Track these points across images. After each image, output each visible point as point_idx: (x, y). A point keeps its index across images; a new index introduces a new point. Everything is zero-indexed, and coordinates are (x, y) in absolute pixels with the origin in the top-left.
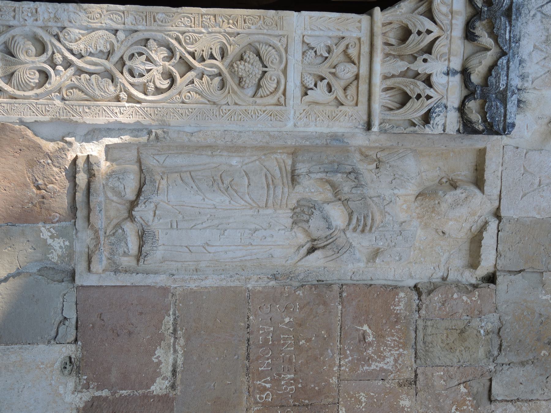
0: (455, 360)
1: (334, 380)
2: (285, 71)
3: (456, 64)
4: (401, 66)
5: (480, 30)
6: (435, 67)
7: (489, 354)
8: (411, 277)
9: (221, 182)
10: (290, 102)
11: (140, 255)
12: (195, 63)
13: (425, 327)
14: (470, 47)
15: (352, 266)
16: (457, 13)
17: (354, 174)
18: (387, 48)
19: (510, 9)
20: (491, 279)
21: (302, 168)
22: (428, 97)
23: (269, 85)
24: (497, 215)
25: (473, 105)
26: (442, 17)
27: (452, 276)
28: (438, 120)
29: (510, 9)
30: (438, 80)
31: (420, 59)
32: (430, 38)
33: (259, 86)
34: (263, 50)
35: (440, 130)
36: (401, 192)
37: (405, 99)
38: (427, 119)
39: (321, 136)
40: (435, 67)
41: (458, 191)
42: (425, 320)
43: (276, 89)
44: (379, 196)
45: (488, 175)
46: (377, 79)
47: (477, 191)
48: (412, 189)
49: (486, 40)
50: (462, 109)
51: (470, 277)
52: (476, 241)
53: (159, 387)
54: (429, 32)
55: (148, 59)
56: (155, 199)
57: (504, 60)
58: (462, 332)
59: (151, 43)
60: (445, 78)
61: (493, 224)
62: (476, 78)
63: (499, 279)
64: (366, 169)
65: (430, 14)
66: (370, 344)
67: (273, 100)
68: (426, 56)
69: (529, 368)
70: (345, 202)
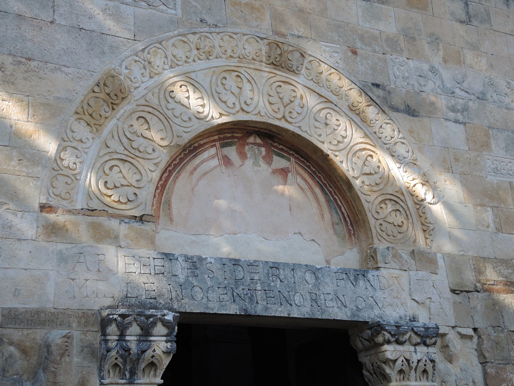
0: (506, 347)
3: (412, 348)
5: (402, 339)
6: (415, 358)
7: (502, 332)
8: (477, 365)
13: (498, 360)
14: (407, 343)
16: (395, 348)
18: (406, 379)
19: (396, 326)
20: (475, 330)
22: (426, 361)
24: (453, 327)
25: (428, 341)
26: (397, 355)
27: (475, 347)
28: (433, 356)
29: (396, 326)
30: (419, 356)
35: (435, 355)
36: (452, 370)
37: (425, 371)
38: (432, 361)
40: (415, 358)
41: (450, 345)
42: (495, 360)
44: (456, 381)
47: (448, 336)
48: (449, 365)
49: (407, 337)
51: (475, 339)
54: (403, 361)
57: (415, 329)
58: (497, 343)
60: (418, 353)
62: (419, 340)
63: (476, 327)
65: (395, 361)
68: (411, 363)
69: (504, 314)
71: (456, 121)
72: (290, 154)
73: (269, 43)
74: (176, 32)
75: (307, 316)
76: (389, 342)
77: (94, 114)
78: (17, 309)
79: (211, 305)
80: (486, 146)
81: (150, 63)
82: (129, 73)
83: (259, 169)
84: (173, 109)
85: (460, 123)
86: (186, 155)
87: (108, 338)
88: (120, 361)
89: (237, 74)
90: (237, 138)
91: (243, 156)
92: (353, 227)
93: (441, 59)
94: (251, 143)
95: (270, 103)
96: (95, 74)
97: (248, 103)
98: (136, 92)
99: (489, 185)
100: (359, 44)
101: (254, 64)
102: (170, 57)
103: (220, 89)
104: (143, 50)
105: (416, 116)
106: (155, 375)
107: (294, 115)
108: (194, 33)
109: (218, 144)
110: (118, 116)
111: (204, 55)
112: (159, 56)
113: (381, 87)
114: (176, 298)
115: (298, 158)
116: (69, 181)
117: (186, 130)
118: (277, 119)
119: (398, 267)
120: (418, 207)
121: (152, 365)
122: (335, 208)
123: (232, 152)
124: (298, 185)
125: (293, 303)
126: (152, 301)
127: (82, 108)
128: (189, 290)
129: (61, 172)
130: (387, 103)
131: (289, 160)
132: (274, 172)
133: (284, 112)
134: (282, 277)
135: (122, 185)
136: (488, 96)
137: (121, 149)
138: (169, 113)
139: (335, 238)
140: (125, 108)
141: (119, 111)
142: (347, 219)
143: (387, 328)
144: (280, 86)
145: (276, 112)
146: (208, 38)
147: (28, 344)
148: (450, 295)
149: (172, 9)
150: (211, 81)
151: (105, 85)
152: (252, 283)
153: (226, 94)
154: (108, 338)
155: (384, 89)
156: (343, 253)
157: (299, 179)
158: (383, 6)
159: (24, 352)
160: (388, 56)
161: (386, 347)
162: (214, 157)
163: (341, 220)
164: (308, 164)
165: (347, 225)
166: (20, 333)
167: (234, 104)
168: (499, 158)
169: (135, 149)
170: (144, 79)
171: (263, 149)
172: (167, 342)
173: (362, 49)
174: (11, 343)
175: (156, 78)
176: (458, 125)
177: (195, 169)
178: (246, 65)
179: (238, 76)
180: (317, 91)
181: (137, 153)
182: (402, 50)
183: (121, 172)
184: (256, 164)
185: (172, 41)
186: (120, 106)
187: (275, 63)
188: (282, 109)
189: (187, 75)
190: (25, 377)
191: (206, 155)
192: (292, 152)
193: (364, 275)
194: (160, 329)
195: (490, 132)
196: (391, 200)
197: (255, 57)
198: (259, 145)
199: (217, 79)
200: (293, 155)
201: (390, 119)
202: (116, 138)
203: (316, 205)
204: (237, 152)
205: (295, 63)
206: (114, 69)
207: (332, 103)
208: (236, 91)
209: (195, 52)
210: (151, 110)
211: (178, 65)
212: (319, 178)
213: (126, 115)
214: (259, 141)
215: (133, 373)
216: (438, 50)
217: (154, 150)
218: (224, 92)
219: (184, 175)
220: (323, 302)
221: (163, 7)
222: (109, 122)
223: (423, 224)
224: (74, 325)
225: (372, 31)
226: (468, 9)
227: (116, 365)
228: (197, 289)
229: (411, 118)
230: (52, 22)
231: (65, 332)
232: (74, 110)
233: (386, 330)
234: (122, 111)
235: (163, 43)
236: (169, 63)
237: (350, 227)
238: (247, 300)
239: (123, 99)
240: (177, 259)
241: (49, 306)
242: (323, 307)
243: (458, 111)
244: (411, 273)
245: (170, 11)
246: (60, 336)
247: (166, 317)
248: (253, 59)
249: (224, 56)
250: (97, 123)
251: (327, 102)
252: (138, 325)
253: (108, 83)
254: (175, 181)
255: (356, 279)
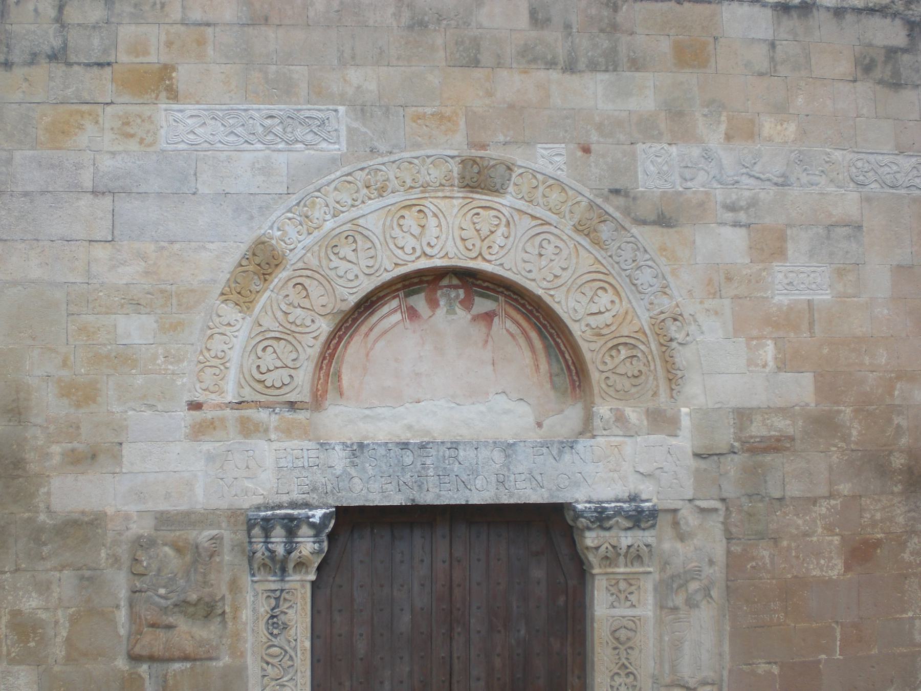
1: (774, 581)
2: (623, 617)
4: (622, 559)
5: (607, 525)
7: (761, 501)
9: (677, 646)
10: (639, 613)
11: (713, 684)
12: (621, 663)
15: (717, 572)
17: (673, 578)
21: (671, 604)
23: (631, 625)
24: (690, 500)
27: (721, 519)
31: (619, 551)
32: (610, 547)
33: (631, 630)
34: (613, 629)
39: (655, 597)
43: (633, 621)
45: (672, 507)
46: (628, 570)
48: (679, 545)
50: (644, 529)
52: (702, 510)
53: (775, 670)
55: (620, 685)
56: (686, 678)
59: (613, 683)
61: (698, 503)
62: (629, 525)
64: (669, 571)
65: (597, 548)
66: (757, 564)
67: (637, 622)
69: (767, 478)
70: (687, 581)
71: (736, 224)
72: (498, 292)
73: (462, 161)
74: (338, 174)
75: (490, 502)
76: (589, 529)
77: (242, 292)
78: (168, 512)
79: (371, 496)
80: (780, 253)
81: (307, 217)
82: (282, 235)
83: (454, 317)
84: (336, 268)
85: (741, 226)
86: (361, 314)
87: (253, 540)
88: (268, 561)
89: (418, 208)
90: (427, 282)
91: (433, 304)
92: (578, 377)
93: (723, 136)
94: (445, 287)
95: (463, 240)
96: (242, 245)
97: (432, 244)
98: (291, 255)
99: (775, 309)
100: (594, 137)
101: (443, 190)
102: (332, 204)
103: (397, 232)
104: (298, 204)
105: (672, 227)
106: (307, 573)
107: (496, 248)
108: (362, 169)
109: (401, 294)
110: (271, 287)
111: (376, 192)
112: (318, 206)
113: (623, 193)
114: (332, 491)
115: (509, 297)
116: (218, 372)
117: (351, 291)
118: (471, 259)
119: (621, 433)
120: (664, 349)
121: (301, 565)
122: (556, 356)
123: (419, 302)
124: (507, 330)
125: (473, 488)
126: (304, 496)
127: (229, 287)
128: (346, 482)
129: (207, 364)
130: (629, 215)
131: (496, 300)
132: (475, 319)
133: (481, 248)
134: (460, 459)
135: (277, 368)
136: (793, 179)
137: (274, 326)
138: (332, 274)
139: (552, 394)
140: (280, 276)
141: (272, 282)
142: (572, 368)
143: (585, 515)
144: (478, 214)
145: (470, 250)
146: (381, 171)
147: (181, 544)
148: (692, 463)
149: (335, 143)
150: (384, 224)
151: (254, 254)
152: (423, 468)
153: (403, 237)
154: (253, 540)
155: (627, 195)
156: (562, 411)
157: (509, 324)
158: (637, 74)
159: (179, 550)
160: (640, 147)
161: (588, 534)
162: (396, 311)
163: (562, 370)
164: (522, 302)
165: (571, 375)
166: (173, 535)
167: (414, 249)
168: (796, 269)
169: (291, 323)
170: (301, 238)
171: (461, 292)
172: (314, 543)
173: (598, 143)
174: (165, 544)
175: (316, 233)
176: (738, 230)
177: (371, 329)
178: (433, 194)
179: (420, 211)
180: (530, 211)
181: (293, 328)
182: (661, 134)
183: (275, 352)
184: (451, 311)
185: (333, 185)
186: (273, 275)
187: (472, 184)
188: (478, 243)
189: (354, 222)
190: (180, 575)
191: (385, 309)
192: (501, 289)
193: (572, 447)
194: (305, 530)
195: (789, 232)
196: (626, 344)
197: (444, 182)
198: (456, 287)
199: (392, 220)
200: (502, 293)
201: (633, 236)
202: (270, 313)
203: (530, 354)
204: (426, 300)
205: (498, 181)
206: (264, 234)
207: (550, 224)
208: (416, 230)
209: (365, 191)
210: (309, 273)
211: (343, 212)
212: (537, 319)
213: (280, 284)
214: (455, 281)
215: (284, 570)
216: (719, 123)
217: (313, 321)
218: (401, 234)
219: (357, 339)
220: (513, 483)
221: (324, 145)
222: (261, 297)
223: (669, 372)
224: (224, 525)
225: (616, 113)
226: (774, 52)
227: (265, 565)
228: (356, 480)
229: (665, 230)
230: (194, 194)
231: (214, 532)
232: (219, 292)
233: (585, 518)
234: (276, 280)
235: (322, 190)
236: (332, 212)
237: (575, 378)
238: (416, 488)
239: (277, 265)
240: (334, 449)
241: (199, 507)
242: (512, 490)
243: (741, 208)
244: (639, 439)
245: (331, 147)
246: (206, 539)
247: (311, 520)
248: (441, 185)
249: (402, 189)
250: (247, 300)
251: (542, 224)
252: (282, 528)
253: (257, 252)
254: (346, 347)
255: (561, 452)
